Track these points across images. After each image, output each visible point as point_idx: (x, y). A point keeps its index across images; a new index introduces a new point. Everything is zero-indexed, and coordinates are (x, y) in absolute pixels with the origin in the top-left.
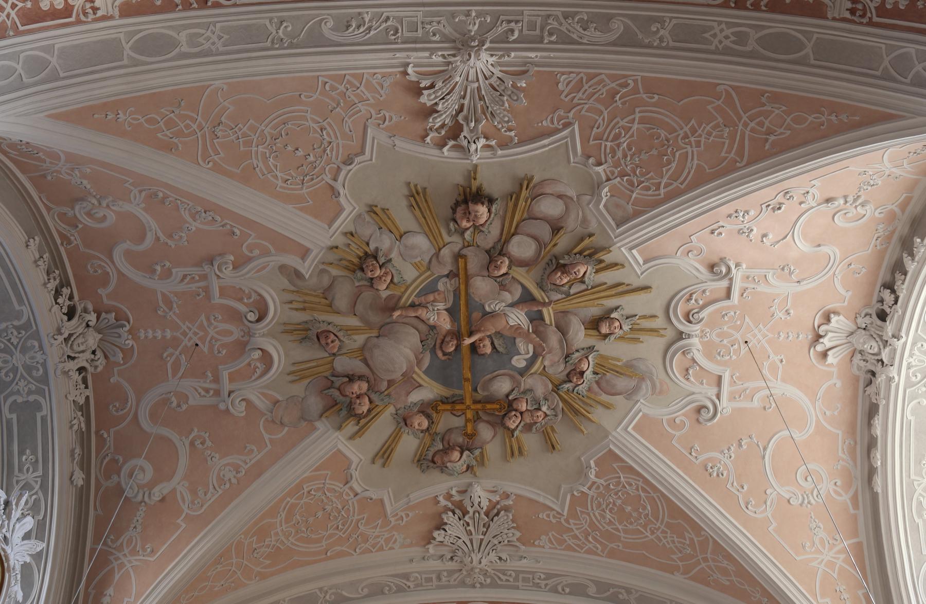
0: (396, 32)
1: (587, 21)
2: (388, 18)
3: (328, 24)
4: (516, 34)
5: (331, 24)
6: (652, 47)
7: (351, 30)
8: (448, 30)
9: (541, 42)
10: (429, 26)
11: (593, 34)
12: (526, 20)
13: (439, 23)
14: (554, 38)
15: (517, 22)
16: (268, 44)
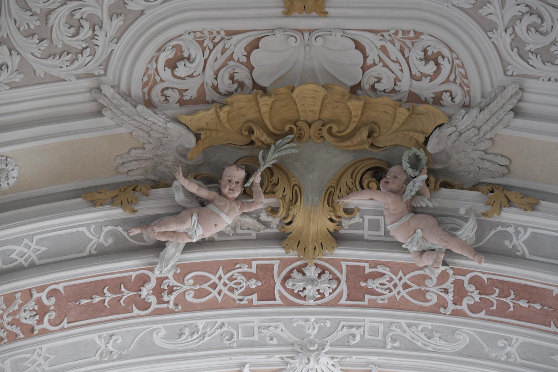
0: (232, 336)
1: (432, 331)
2: (223, 325)
3: (160, 334)
4: (358, 339)
5: (163, 333)
6: (499, 361)
7: (184, 337)
8: (286, 335)
9: (385, 347)
10: (266, 331)
11: (437, 342)
12: (367, 325)
13: (276, 327)
14: (397, 344)
15: (358, 327)
16: (97, 358)
